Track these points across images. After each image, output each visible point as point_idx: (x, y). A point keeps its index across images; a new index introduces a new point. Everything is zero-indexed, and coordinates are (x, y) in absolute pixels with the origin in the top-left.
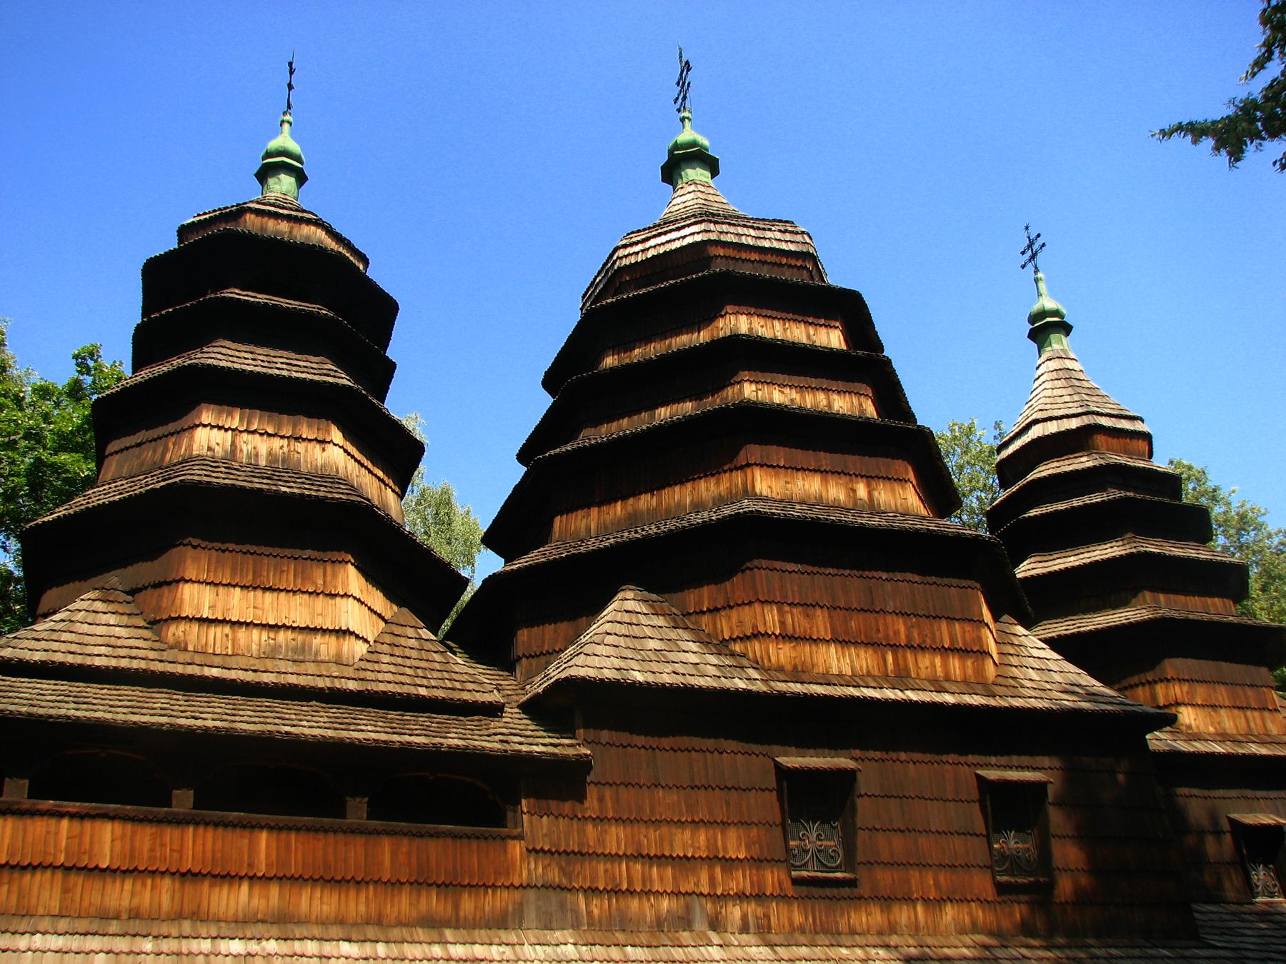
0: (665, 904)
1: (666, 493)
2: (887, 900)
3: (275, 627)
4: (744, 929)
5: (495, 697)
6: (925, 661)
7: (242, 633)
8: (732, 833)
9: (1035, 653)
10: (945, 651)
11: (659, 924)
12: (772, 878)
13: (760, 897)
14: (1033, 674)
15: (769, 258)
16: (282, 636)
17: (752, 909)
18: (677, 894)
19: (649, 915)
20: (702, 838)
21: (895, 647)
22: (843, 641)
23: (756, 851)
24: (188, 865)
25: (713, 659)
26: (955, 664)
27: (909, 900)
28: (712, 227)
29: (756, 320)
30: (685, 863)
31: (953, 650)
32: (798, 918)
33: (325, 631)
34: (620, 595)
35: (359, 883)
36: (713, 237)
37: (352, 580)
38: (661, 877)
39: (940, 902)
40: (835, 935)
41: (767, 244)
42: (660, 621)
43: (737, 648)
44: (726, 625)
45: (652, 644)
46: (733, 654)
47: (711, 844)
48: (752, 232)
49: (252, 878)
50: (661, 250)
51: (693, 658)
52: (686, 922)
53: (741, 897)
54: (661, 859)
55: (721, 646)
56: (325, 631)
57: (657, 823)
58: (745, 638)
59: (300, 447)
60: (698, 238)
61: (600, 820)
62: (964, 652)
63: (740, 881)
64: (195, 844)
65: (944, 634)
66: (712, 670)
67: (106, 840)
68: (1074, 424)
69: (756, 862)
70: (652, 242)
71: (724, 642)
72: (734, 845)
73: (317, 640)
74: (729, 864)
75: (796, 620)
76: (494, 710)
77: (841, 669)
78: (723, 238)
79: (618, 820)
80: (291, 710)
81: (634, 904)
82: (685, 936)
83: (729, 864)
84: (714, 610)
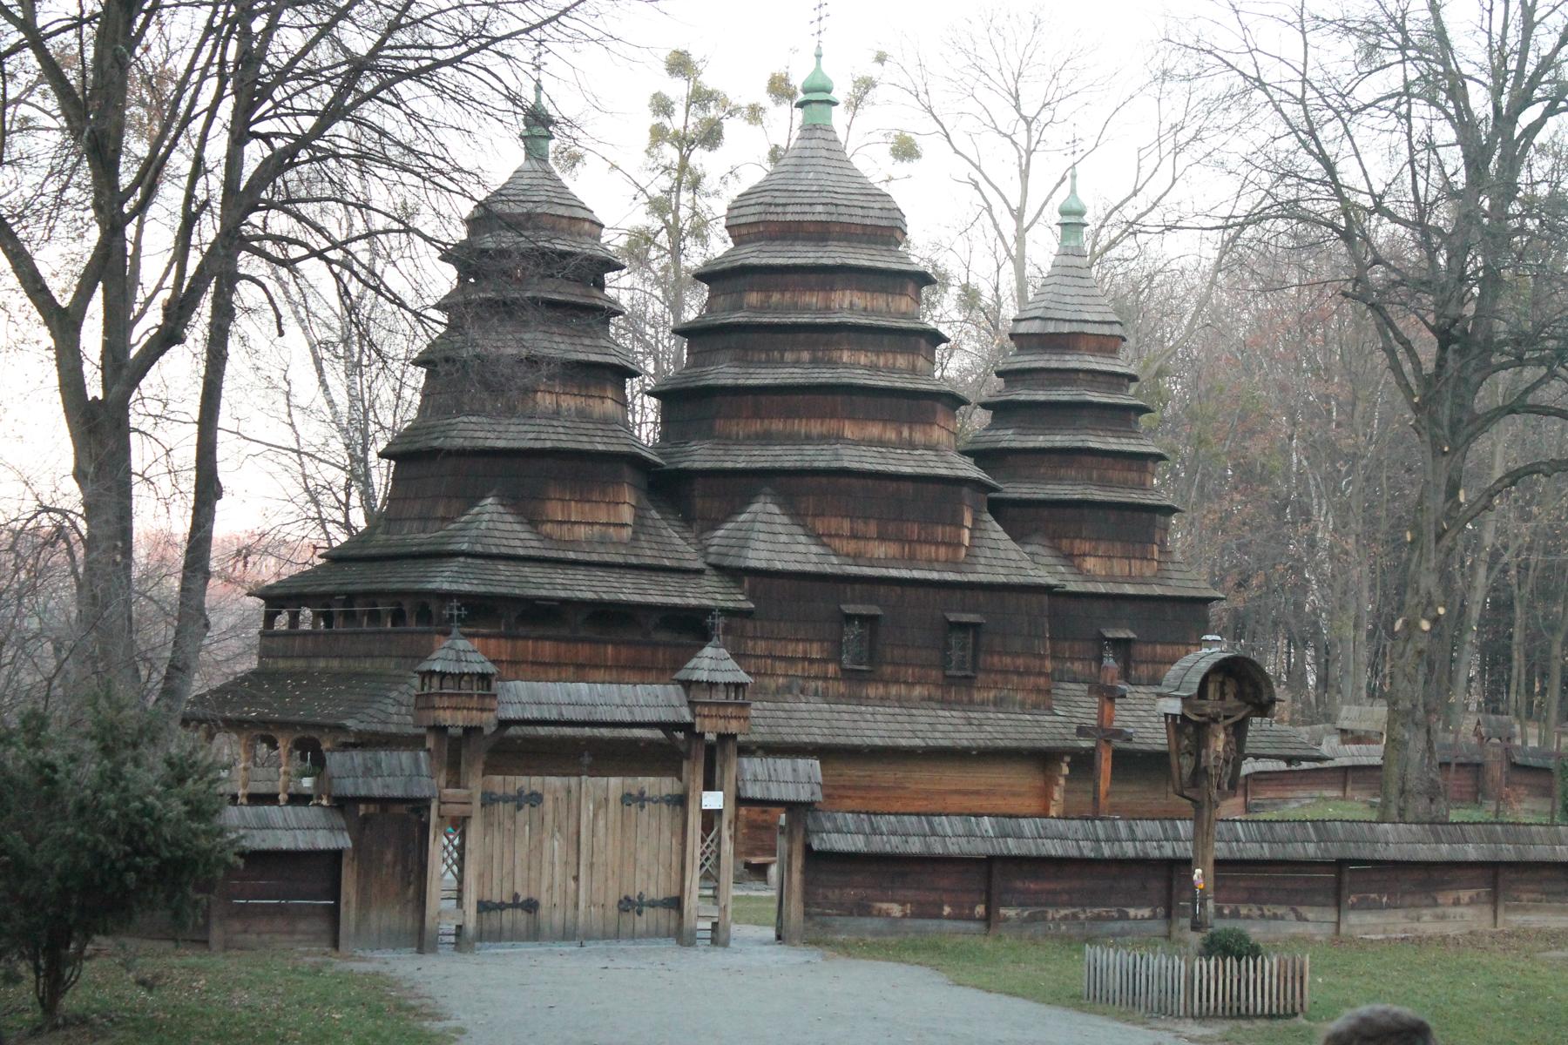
0: (781, 680)
1: (789, 422)
2: (886, 683)
3: (592, 524)
4: (816, 694)
5: (699, 565)
6: (926, 551)
7: (576, 527)
8: (816, 646)
9: (994, 536)
10: (937, 544)
11: (778, 691)
12: (831, 669)
13: (826, 678)
14: (988, 553)
15: (869, 230)
16: (596, 528)
17: (820, 683)
18: (786, 676)
19: (773, 686)
20: (801, 647)
21: (911, 542)
22: (882, 538)
23: (825, 655)
24: (581, 660)
25: (814, 549)
26: (942, 551)
27: (897, 682)
28: (833, 209)
29: (856, 293)
30: (791, 660)
31: (943, 543)
32: (842, 689)
33: (615, 525)
34: (762, 498)
35: (650, 669)
36: (834, 218)
37: (628, 495)
38: (780, 667)
39: (913, 684)
40: (861, 700)
41: (868, 222)
42: (786, 520)
43: (825, 540)
44: (820, 526)
45: (783, 538)
46: (824, 545)
47: (805, 652)
48: (860, 212)
49: (606, 667)
50: (797, 218)
51: (801, 548)
52: (788, 689)
53: (816, 678)
54: (781, 658)
55: (816, 537)
56: (615, 525)
57: (780, 639)
58: (830, 536)
59: (591, 401)
60: (823, 218)
61: (754, 638)
62: (948, 544)
63: (815, 670)
64: (584, 651)
65: (939, 532)
66: (814, 559)
67: (547, 649)
68: (1066, 328)
69: (824, 661)
70: (790, 209)
71: (819, 536)
72: (815, 651)
73: (611, 530)
74: (812, 661)
75: (860, 526)
76: (699, 572)
77: (881, 559)
78: (842, 219)
79: (762, 638)
80: (612, 578)
81: (767, 680)
82: (789, 698)
83: (812, 661)
84: (815, 516)
